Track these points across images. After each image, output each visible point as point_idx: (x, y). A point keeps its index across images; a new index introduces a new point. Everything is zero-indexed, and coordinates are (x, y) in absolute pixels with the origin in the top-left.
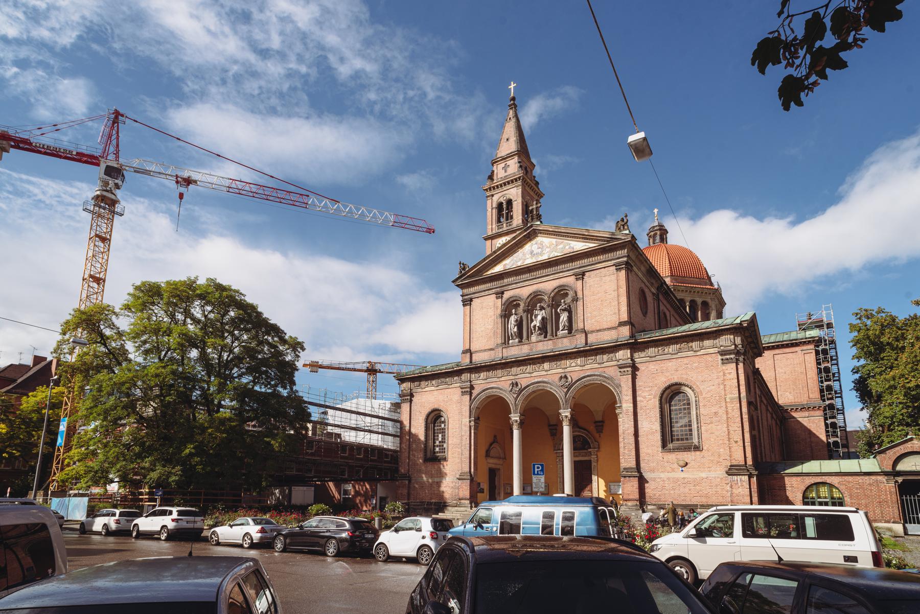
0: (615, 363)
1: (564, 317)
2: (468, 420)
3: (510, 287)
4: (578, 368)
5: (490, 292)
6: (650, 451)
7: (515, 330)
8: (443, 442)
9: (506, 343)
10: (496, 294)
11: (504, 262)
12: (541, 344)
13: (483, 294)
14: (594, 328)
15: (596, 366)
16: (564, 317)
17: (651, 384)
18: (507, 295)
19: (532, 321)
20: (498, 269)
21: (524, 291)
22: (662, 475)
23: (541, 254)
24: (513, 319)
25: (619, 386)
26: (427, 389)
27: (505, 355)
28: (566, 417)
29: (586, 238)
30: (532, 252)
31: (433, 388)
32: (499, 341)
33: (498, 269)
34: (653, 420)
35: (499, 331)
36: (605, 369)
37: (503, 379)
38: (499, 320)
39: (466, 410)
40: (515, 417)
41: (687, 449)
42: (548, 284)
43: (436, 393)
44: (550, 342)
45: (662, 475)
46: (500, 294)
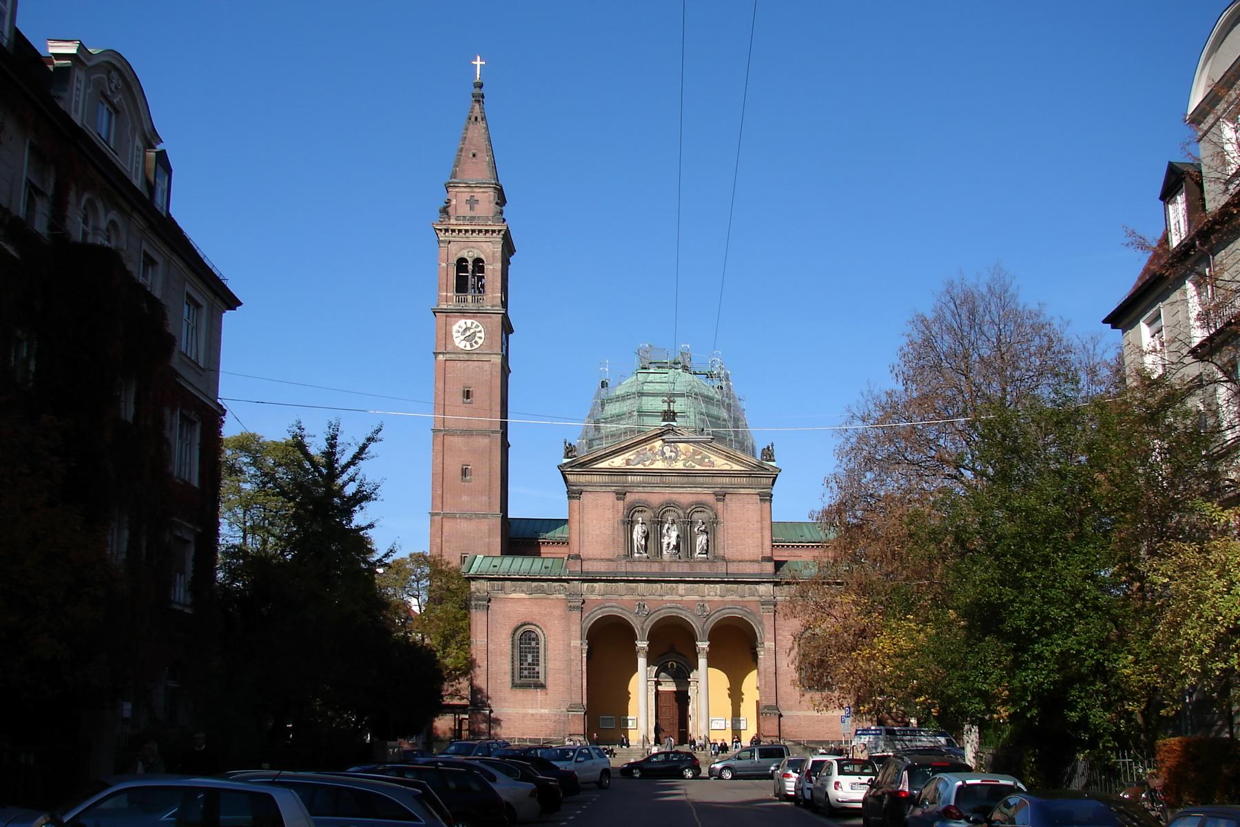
1: (701, 540)
5: (608, 489)
8: (536, 662)
9: (629, 555)
11: (626, 456)
12: (675, 565)
13: (598, 489)
14: (735, 558)
16: (701, 540)
18: (630, 498)
19: (662, 536)
20: (618, 462)
21: (657, 497)
23: (676, 460)
24: (638, 531)
25: (761, 623)
26: (514, 595)
27: (629, 569)
30: (663, 453)
31: (523, 595)
32: (622, 552)
33: (618, 462)
37: (625, 598)
38: (621, 527)
39: (576, 630)
40: (642, 644)
42: (685, 496)
46: (621, 495)
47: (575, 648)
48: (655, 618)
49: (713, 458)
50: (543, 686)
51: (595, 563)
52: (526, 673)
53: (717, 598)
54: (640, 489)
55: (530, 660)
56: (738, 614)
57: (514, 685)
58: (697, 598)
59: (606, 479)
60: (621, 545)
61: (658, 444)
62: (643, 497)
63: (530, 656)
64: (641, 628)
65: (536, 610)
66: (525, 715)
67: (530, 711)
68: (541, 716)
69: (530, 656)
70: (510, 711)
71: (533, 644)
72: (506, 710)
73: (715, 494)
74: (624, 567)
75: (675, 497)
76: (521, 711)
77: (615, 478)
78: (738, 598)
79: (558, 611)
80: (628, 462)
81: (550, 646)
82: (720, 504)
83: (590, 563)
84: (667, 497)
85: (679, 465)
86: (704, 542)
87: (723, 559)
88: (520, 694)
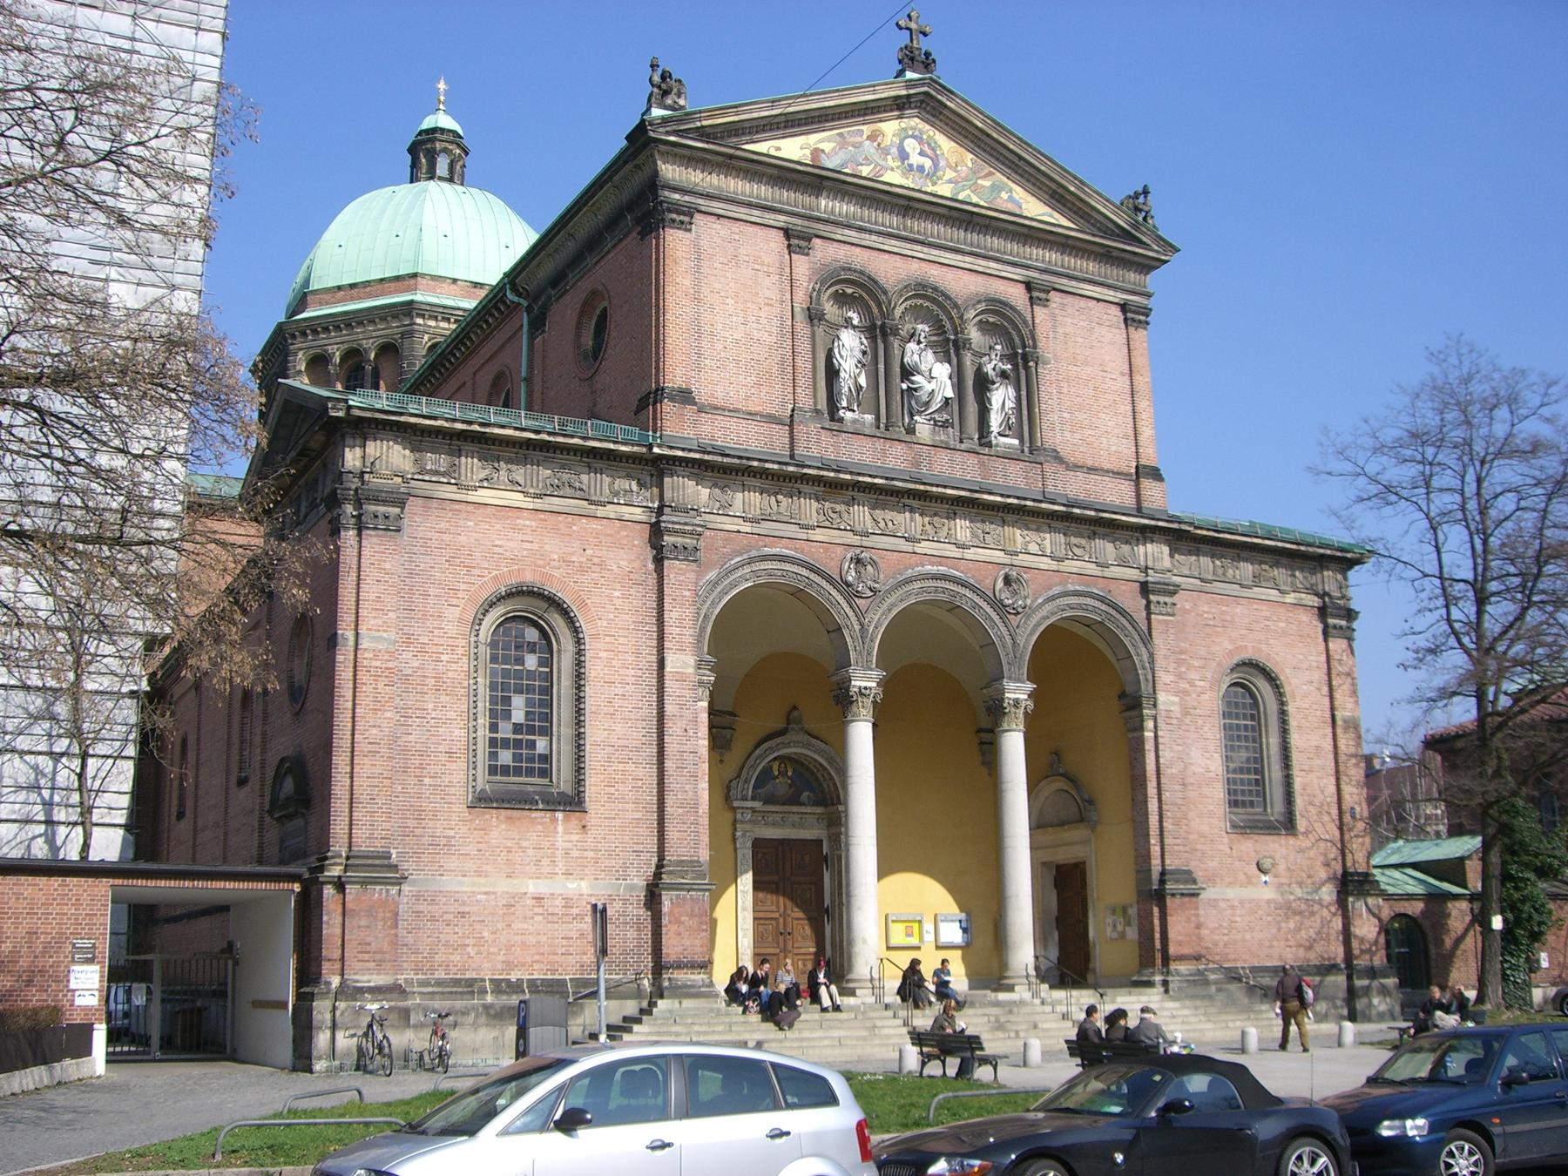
0: (1134, 574)
1: (1001, 397)
2: (692, 661)
3: (839, 233)
4: (1045, 563)
5: (770, 218)
6: (1205, 828)
7: (862, 381)
8: (541, 721)
10: (787, 233)
11: (813, 139)
12: (944, 456)
13: (742, 212)
14: (1077, 458)
15: (1091, 569)
17: (1203, 652)
18: (824, 252)
21: (892, 267)
22: (1232, 893)
25: (1147, 638)
26: (484, 495)
27: (831, 455)
28: (1017, 702)
29: (1057, 196)
30: (903, 155)
31: (516, 499)
32: (805, 401)
33: (793, 148)
34: (1211, 748)
35: (804, 364)
36: (1113, 586)
37: (819, 535)
38: (802, 328)
40: (865, 680)
41: (1269, 828)
42: (964, 278)
43: (527, 521)
44: (972, 460)
45: (1232, 893)
46: (797, 240)
47: (681, 678)
48: (896, 603)
49: (1019, 193)
50: (574, 802)
51: (732, 424)
52: (506, 757)
53: (1045, 563)
54: (851, 235)
55: (518, 716)
56: (1095, 610)
57: (482, 801)
58: (998, 556)
59: (761, 191)
60: (804, 381)
61: (890, 128)
62: (860, 258)
63: (518, 702)
64: (867, 629)
65: (553, 547)
66: (511, 903)
67: (532, 887)
68: (568, 902)
69: (518, 702)
70: (465, 886)
71: (531, 662)
72: (449, 883)
73: (1029, 286)
74: (818, 446)
75: (935, 274)
76: (503, 886)
77: (786, 196)
78: (1091, 569)
79: (627, 554)
80: (816, 152)
81: (593, 670)
82: (1041, 313)
83: (720, 420)
84: (915, 270)
85: (945, 190)
86: (1010, 404)
87: (1058, 458)
88: (500, 827)
